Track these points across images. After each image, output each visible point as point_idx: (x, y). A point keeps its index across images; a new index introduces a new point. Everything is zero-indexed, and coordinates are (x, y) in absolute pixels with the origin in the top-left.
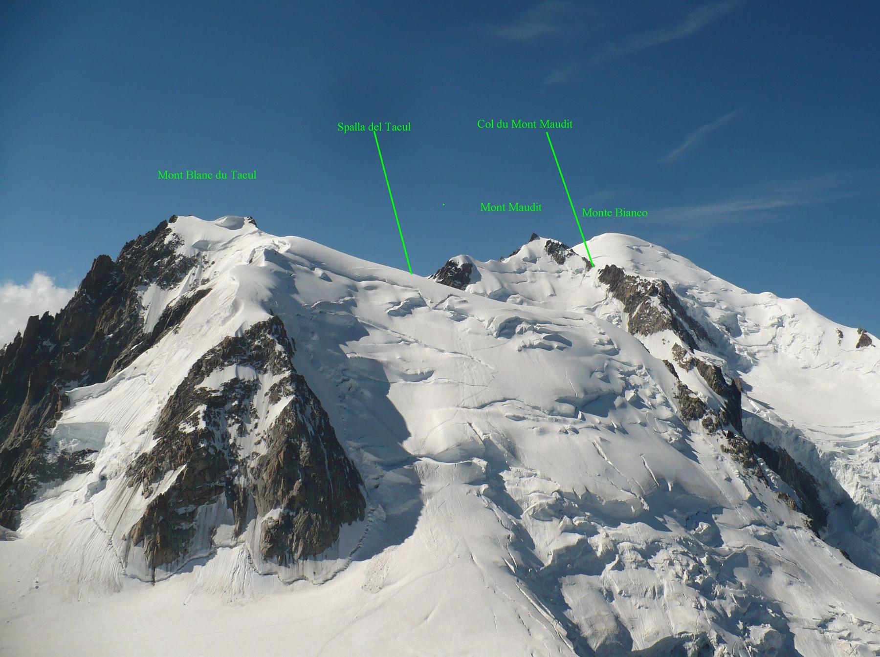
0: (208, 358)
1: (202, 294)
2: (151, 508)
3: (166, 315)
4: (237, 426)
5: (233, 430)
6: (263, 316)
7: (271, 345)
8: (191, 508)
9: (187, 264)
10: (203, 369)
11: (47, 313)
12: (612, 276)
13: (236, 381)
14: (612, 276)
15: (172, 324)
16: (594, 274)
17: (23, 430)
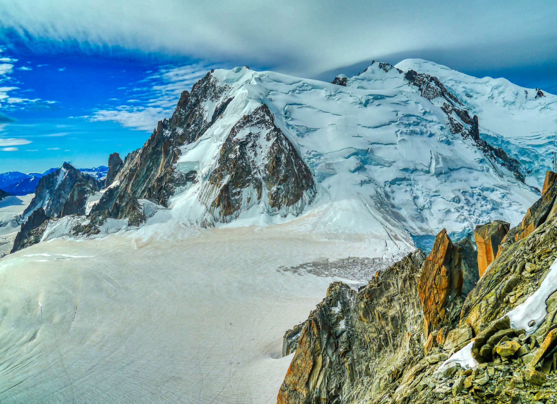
0: (238, 125)
1: (230, 100)
2: (222, 191)
3: (216, 111)
4: (253, 153)
5: (252, 155)
6: (259, 105)
7: (264, 116)
8: (238, 190)
9: (222, 90)
10: (236, 130)
11: (165, 120)
12: (411, 76)
13: (250, 134)
14: (411, 76)
15: (220, 114)
16: (403, 75)
17: (163, 169)
